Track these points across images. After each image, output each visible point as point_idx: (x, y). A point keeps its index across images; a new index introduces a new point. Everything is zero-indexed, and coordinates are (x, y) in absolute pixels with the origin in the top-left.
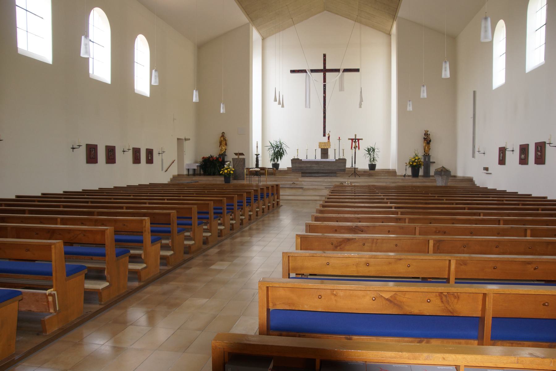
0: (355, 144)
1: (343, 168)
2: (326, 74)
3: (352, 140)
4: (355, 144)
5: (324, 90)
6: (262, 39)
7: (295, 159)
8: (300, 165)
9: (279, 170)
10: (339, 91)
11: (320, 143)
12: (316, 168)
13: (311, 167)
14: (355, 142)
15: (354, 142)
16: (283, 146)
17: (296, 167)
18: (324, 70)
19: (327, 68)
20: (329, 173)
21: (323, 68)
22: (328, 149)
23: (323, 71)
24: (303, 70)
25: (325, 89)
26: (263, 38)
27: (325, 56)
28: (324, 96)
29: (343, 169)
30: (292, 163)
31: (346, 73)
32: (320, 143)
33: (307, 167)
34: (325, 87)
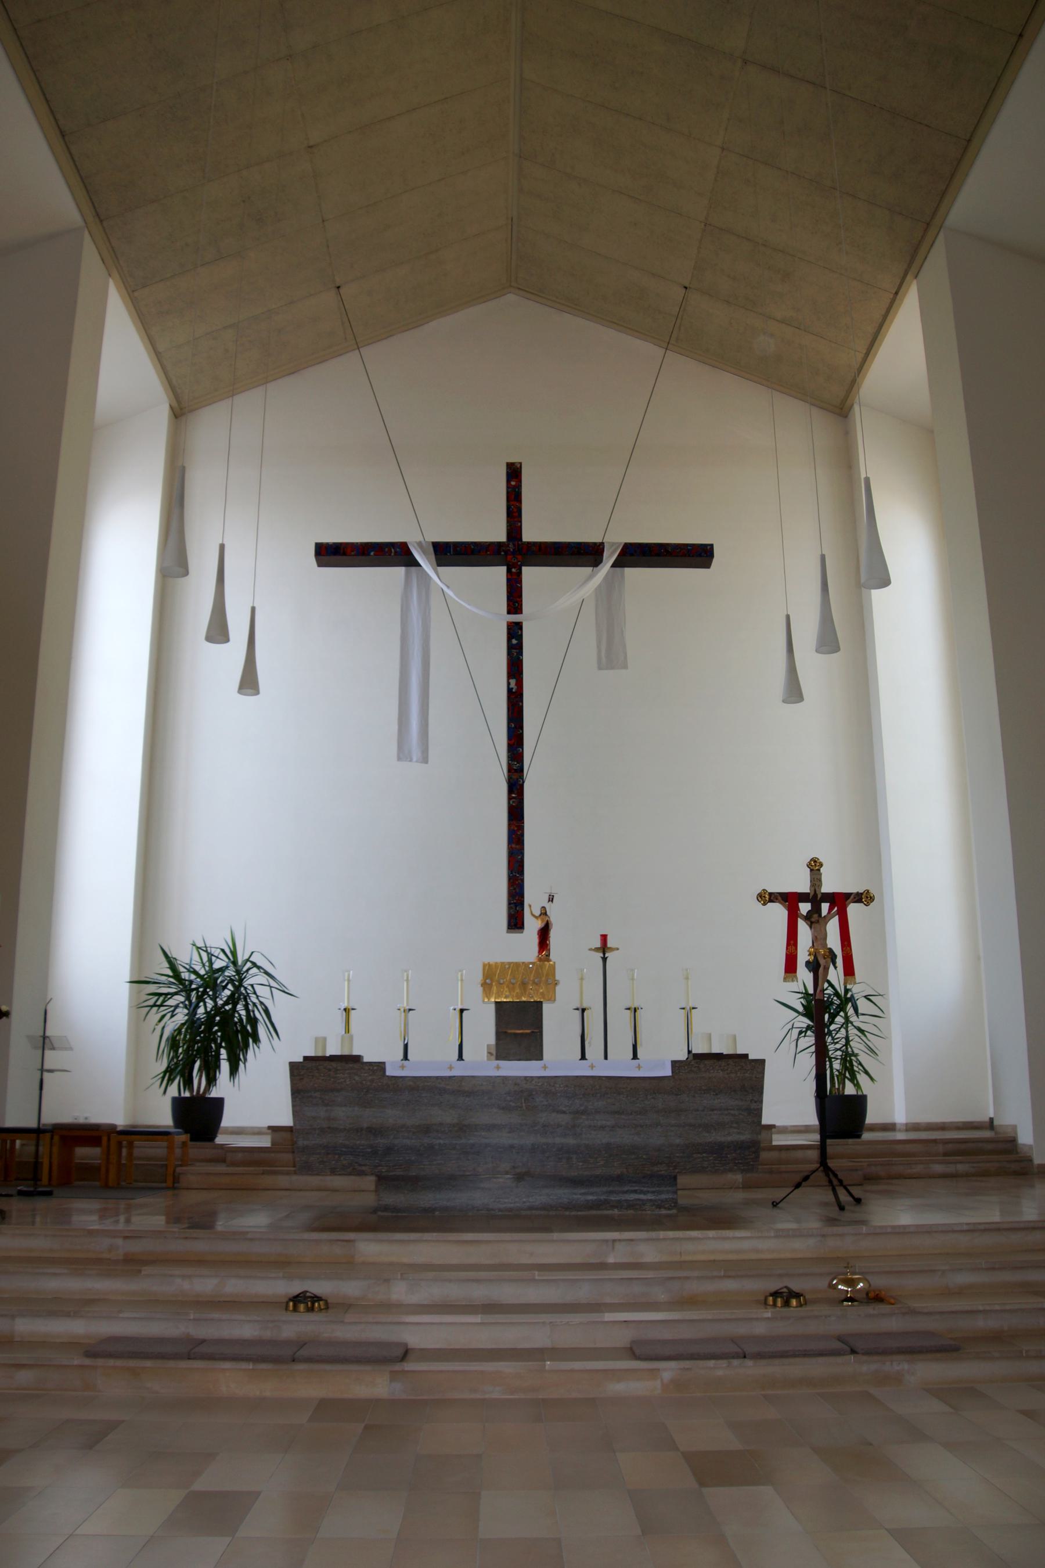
0: (819, 939)
2: (520, 573)
3: (791, 900)
4: (819, 939)
8: (369, 1117)
9: (220, 1139)
10: (600, 668)
12: (504, 1139)
13: (463, 1129)
14: (814, 919)
15: (808, 918)
16: (254, 979)
19: (530, 534)
20: (620, 1179)
23: (507, 552)
24: (392, 545)
28: (510, 691)
30: (298, 1093)
31: (633, 574)
33: (426, 1129)
34: (520, 638)
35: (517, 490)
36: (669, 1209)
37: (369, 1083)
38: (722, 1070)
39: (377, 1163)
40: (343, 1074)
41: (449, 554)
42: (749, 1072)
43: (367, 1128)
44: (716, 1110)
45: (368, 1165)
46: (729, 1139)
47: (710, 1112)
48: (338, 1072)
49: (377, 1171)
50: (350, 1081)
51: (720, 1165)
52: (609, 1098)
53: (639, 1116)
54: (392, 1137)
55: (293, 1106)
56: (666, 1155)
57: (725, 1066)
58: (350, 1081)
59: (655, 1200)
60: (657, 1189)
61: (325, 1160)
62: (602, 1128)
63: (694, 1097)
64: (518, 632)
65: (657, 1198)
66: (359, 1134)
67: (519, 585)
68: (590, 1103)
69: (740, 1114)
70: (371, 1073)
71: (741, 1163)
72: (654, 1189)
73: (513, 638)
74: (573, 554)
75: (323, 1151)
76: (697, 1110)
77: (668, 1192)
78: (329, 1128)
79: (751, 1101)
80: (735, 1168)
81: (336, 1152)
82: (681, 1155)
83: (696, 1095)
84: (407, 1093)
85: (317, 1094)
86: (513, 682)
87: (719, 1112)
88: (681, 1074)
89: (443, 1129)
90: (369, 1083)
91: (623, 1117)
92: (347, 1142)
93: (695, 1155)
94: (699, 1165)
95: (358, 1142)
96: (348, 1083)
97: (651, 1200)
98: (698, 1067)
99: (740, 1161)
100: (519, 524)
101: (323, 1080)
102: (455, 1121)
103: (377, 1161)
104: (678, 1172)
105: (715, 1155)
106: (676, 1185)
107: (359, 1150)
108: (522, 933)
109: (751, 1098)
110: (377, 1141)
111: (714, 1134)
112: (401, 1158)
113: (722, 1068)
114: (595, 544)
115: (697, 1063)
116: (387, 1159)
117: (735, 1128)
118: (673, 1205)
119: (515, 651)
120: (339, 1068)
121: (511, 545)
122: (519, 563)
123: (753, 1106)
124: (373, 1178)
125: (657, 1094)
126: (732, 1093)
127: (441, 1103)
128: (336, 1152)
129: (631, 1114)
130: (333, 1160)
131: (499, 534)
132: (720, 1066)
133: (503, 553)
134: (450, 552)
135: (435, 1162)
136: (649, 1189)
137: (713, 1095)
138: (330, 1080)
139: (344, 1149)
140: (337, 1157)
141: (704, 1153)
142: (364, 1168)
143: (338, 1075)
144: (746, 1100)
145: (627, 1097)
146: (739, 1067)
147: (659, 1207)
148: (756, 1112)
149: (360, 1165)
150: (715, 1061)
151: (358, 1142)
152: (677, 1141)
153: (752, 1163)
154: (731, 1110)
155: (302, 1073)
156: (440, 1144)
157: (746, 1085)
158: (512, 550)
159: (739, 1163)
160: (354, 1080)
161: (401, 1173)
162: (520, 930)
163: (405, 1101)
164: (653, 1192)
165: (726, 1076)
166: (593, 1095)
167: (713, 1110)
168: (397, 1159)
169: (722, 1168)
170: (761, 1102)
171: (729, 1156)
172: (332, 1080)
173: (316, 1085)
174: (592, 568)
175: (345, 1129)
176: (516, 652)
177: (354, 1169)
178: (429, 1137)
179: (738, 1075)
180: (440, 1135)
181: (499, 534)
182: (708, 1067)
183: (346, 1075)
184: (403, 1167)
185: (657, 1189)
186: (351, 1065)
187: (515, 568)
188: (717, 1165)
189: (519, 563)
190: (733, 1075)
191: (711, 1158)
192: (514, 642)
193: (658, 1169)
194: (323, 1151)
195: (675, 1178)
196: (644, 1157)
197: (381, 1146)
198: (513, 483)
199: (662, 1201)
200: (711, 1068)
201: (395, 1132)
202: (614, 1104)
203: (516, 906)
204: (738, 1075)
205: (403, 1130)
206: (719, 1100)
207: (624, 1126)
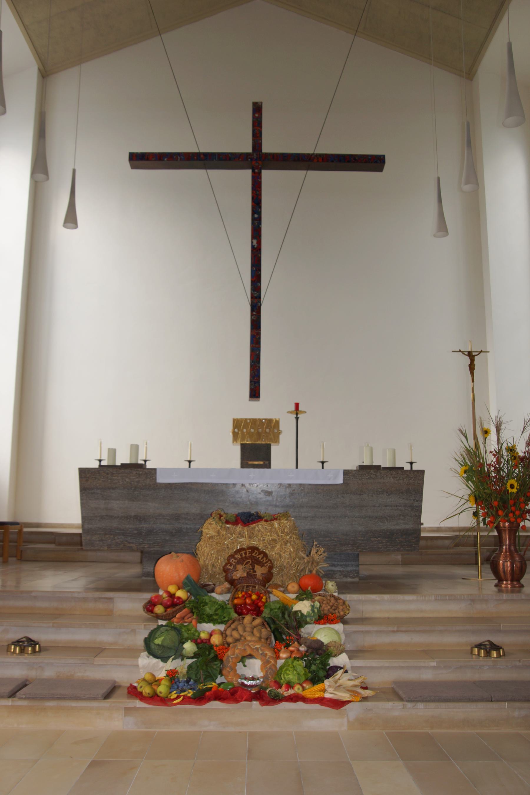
1: (402, 525)
2: (260, 173)
5: (253, 223)
6: (39, 69)
7: (114, 467)
11: (238, 424)
17: (111, 517)
18: (255, 156)
19: (267, 148)
21: (248, 149)
22: (270, 445)
23: (252, 159)
25: (256, 222)
26: (42, 68)
27: (257, 109)
28: (253, 247)
29: (405, 533)
30: (84, 490)
32: (238, 424)
33: (177, 517)
35: (259, 120)
36: (353, 578)
37: (136, 484)
38: (393, 477)
39: (142, 541)
40: (118, 477)
41: (215, 160)
42: (412, 479)
43: (135, 516)
44: (388, 506)
45: (135, 543)
46: (398, 527)
47: (384, 508)
48: (114, 475)
49: (141, 547)
50: (122, 482)
51: (390, 546)
52: (310, 496)
53: (332, 510)
54: (152, 523)
55: (82, 499)
56: (351, 539)
57: (395, 474)
58: (122, 482)
59: (343, 571)
60: (345, 563)
61: (104, 538)
62: (306, 518)
63: (372, 496)
64: (258, 210)
65: (344, 570)
66: (128, 520)
67: (260, 180)
68: (297, 500)
69: (406, 510)
70: (137, 476)
71: (406, 545)
72: (342, 563)
73: (255, 213)
74: (294, 160)
75: (102, 532)
76: (374, 506)
77: (352, 565)
78: (107, 516)
79: (414, 500)
80: (402, 548)
81: (112, 533)
82: (362, 538)
83: (374, 495)
84: (163, 491)
85: (99, 491)
86: (255, 242)
87: (390, 508)
88: (363, 479)
89: (189, 517)
90: (136, 484)
91: (320, 510)
92: (120, 526)
93: (372, 539)
94: (376, 546)
95: (128, 526)
96: (121, 483)
97: (340, 571)
98: (376, 475)
99: (405, 544)
100: (260, 141)
101: (103, 481)
102: (198, 512)
103: (141, 540)
104: (360, 551)
105: (386, 539)
106: (358, 560)
107: (128, 532)
108: (259, 401)
109: (414, 498)
110: (141, 526)
111: (386, 524)
112: (158, 538)
113: (393, 476)
114: (309, 154)
115: (375, 472)
116: (148, 538)
117: (402, 520)
118: (356, 575)
119: (256, 222)
120: (114, 472)
121: (255, 155)
122: (260, 166)
123: (416, 504)
124: (139, 554)
125: (345, 494)
126: (400, 494)
127: (188, 498)
128: (112, 533)
129: (326, 508)
130: (109, 539)
131: (247, 148)
132: (392, 474)
133: (249, 160)
134: (215, 159)
135: (183, 542)
136: (339, 563)
137: (387, 495)
138: (108, 481)
139: (117, 531)
140: (112, 536)
141: (379, 537)
142: (131, 545)
143: (114, 478)
144: (410, 500)
145: (324, 495)
146: (406, 476)
147: (346, 576)
148: (417, 508)
149: (129, 543)
150: (388, 470)
151: (128, 526)
152: (360, 528)
153: (414, 545)
154: (399, 506)
155: (88, 476)
156: (187, 528)
157: (410, 489)
158: (255, 158)
159: (404, 545)
160: (126, 481)
161: (159, 549)
162: (255, 399)
163: (162, 497)
164: (341, 565)
165: (396, 482)
166: (299, 494)
167: (386, 506)
168: (155, 538)
169: (392, 549)
170: (421, 501)
171: (397, 540)
172: (109, 481)
173: (97, 485)
174: (306, 171)
175: (119, 517)
176: (257, 223)
177: (124, 545)
178: (179, 523)
179: (405, 481)
180: (187, 522)
181: (247, 148)
182: (383, 475)
183: (119, 478)
184: (160, 544)
185: (345, 563)
186: (123, 470)
187: (257, 169)
188: (388, 546)
189: (260, 166)
190: (401, 481)
191: (385, 541)
192: (256, 216)
193: (346, 548)
194: (102, 532)
195: (358, 555)
196: (335, 539)
197: (144, 529)
198: (257, 115)
199: (348, 572)
200: (385, 476)
201: (155, 520)
202: (314, 501)
203: (255, 384)
204: (405, 481)
205: (161, 517)
206: (391, 499)
207: (321, 517)
